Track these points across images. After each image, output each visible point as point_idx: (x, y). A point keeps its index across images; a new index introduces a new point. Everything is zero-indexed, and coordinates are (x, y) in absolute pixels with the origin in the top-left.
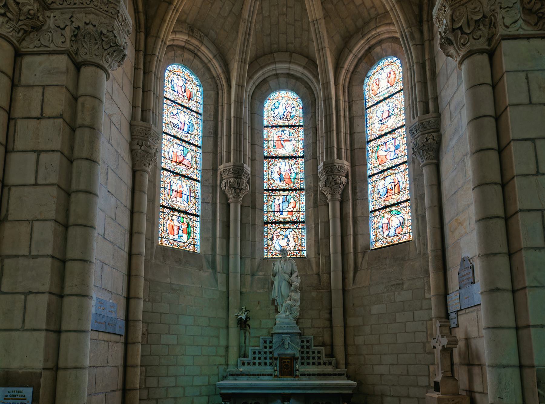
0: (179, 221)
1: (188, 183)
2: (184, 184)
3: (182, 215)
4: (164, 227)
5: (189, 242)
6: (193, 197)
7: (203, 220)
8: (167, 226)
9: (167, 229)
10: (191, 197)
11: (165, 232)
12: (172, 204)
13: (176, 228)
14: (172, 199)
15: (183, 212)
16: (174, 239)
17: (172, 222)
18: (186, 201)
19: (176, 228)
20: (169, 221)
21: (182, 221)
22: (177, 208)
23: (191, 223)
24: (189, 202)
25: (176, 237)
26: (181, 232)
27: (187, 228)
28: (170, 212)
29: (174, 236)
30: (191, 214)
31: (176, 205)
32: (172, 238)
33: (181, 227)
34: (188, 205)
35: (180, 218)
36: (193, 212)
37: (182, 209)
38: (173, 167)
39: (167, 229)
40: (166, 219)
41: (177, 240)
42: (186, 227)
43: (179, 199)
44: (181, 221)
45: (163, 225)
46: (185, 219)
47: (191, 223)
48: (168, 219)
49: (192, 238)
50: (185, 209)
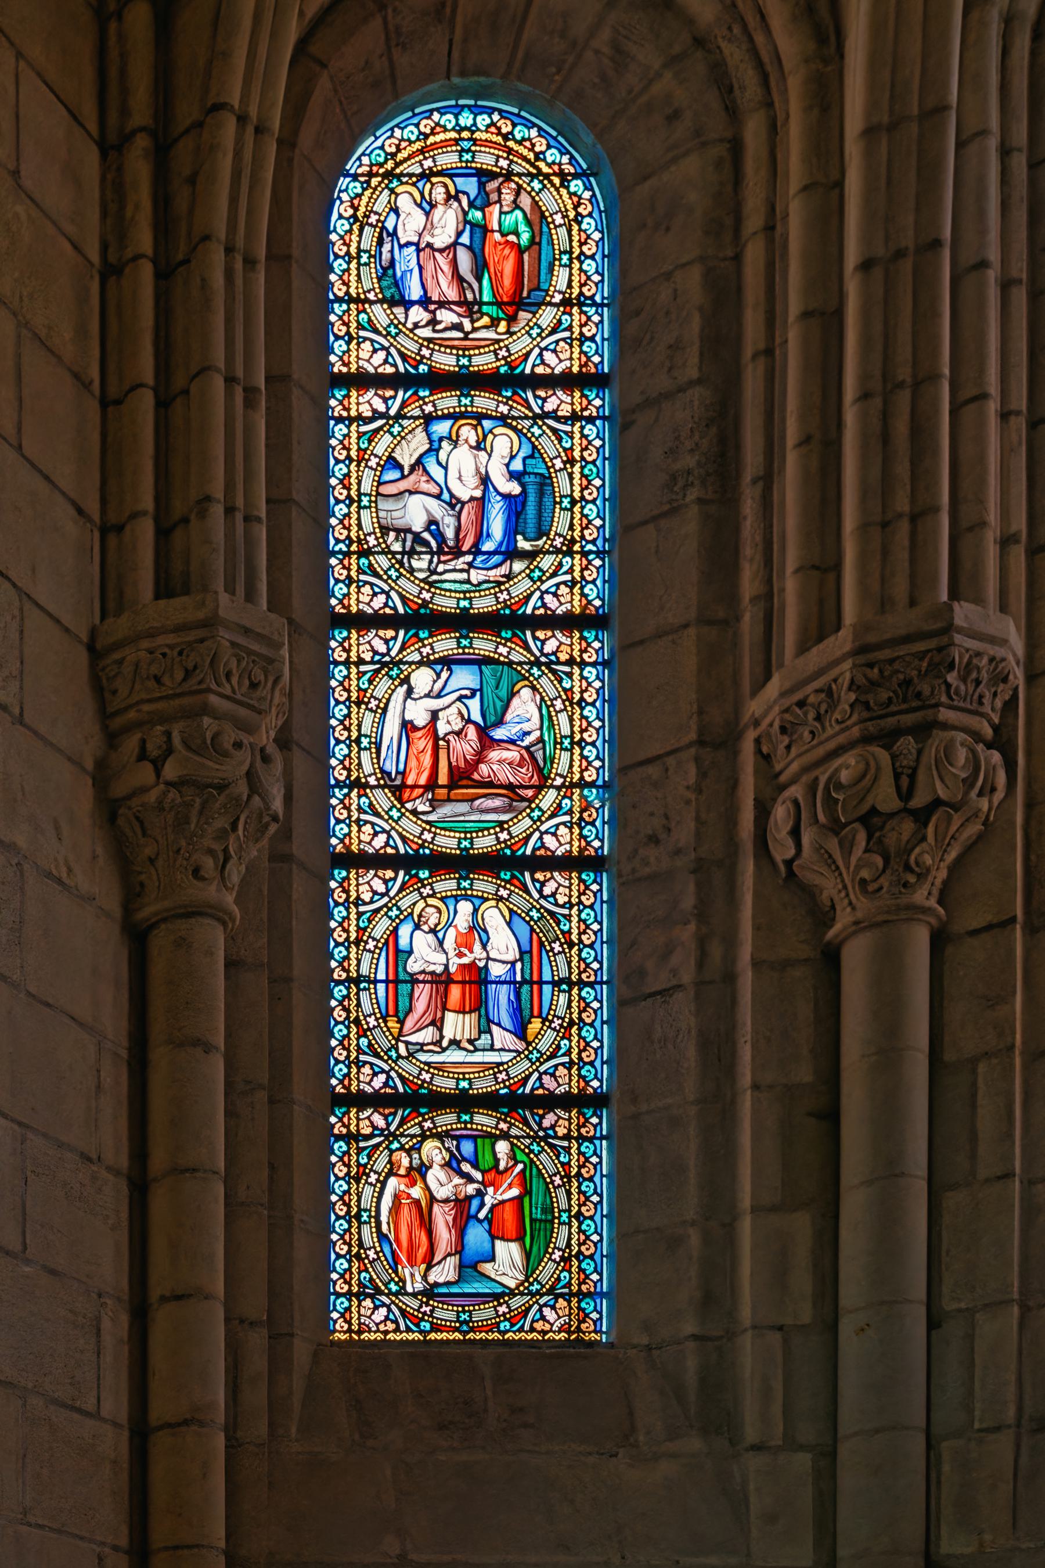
0: (466, 1167)
1: (519, 901)
2: (493, 918)
3: (484, 1120)
4: (365, 1229)
5: (536, 1287)
6: (555, 984)
7: (636, 1117)
8: (384, 1218)
9: (382, 1237)
10: (547, 989)
11: (372, 1254)
12: (409, 1068)
13: (442, 1218)
14: (412, 1039)
15: (490, 1101)
16: (436, 1285)
17: (413, 1184)
18: (506, 1022)
19: (442, 1218)
20: (392, 1182)
21: (487, 1161)
22: (445, 1084)
23: (546, 1161)
24: (535, 1025)
25: (444, 1272)
26: (476, 1236)
27: (518, 1200)
28: (403, 1122)
29: (429, 1267)
30: (551, 1102)
31: (440, 1067)
32: (419, 1286)
33: (475, 1203)
34: (520, 1046)
35: (467, 1147)
36: (562, 1084)
37: (483, 1085)
38: (411, 827)
39: (382, 1237)
40: (373, 1178)
41: (455, 1290)
42: (515, 1192)
43: (456, 1025)
44: (475, 1165)
45: (358, 1216)
46: (502, 1147)
47: (546, 1161)
48: (391, 1173)
49: (557, 1255)
50: (502, 1076)
